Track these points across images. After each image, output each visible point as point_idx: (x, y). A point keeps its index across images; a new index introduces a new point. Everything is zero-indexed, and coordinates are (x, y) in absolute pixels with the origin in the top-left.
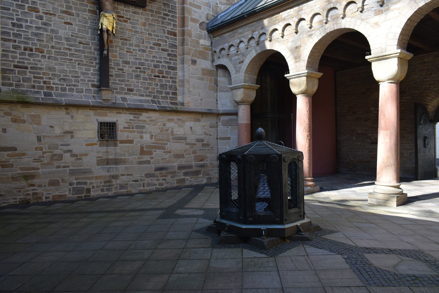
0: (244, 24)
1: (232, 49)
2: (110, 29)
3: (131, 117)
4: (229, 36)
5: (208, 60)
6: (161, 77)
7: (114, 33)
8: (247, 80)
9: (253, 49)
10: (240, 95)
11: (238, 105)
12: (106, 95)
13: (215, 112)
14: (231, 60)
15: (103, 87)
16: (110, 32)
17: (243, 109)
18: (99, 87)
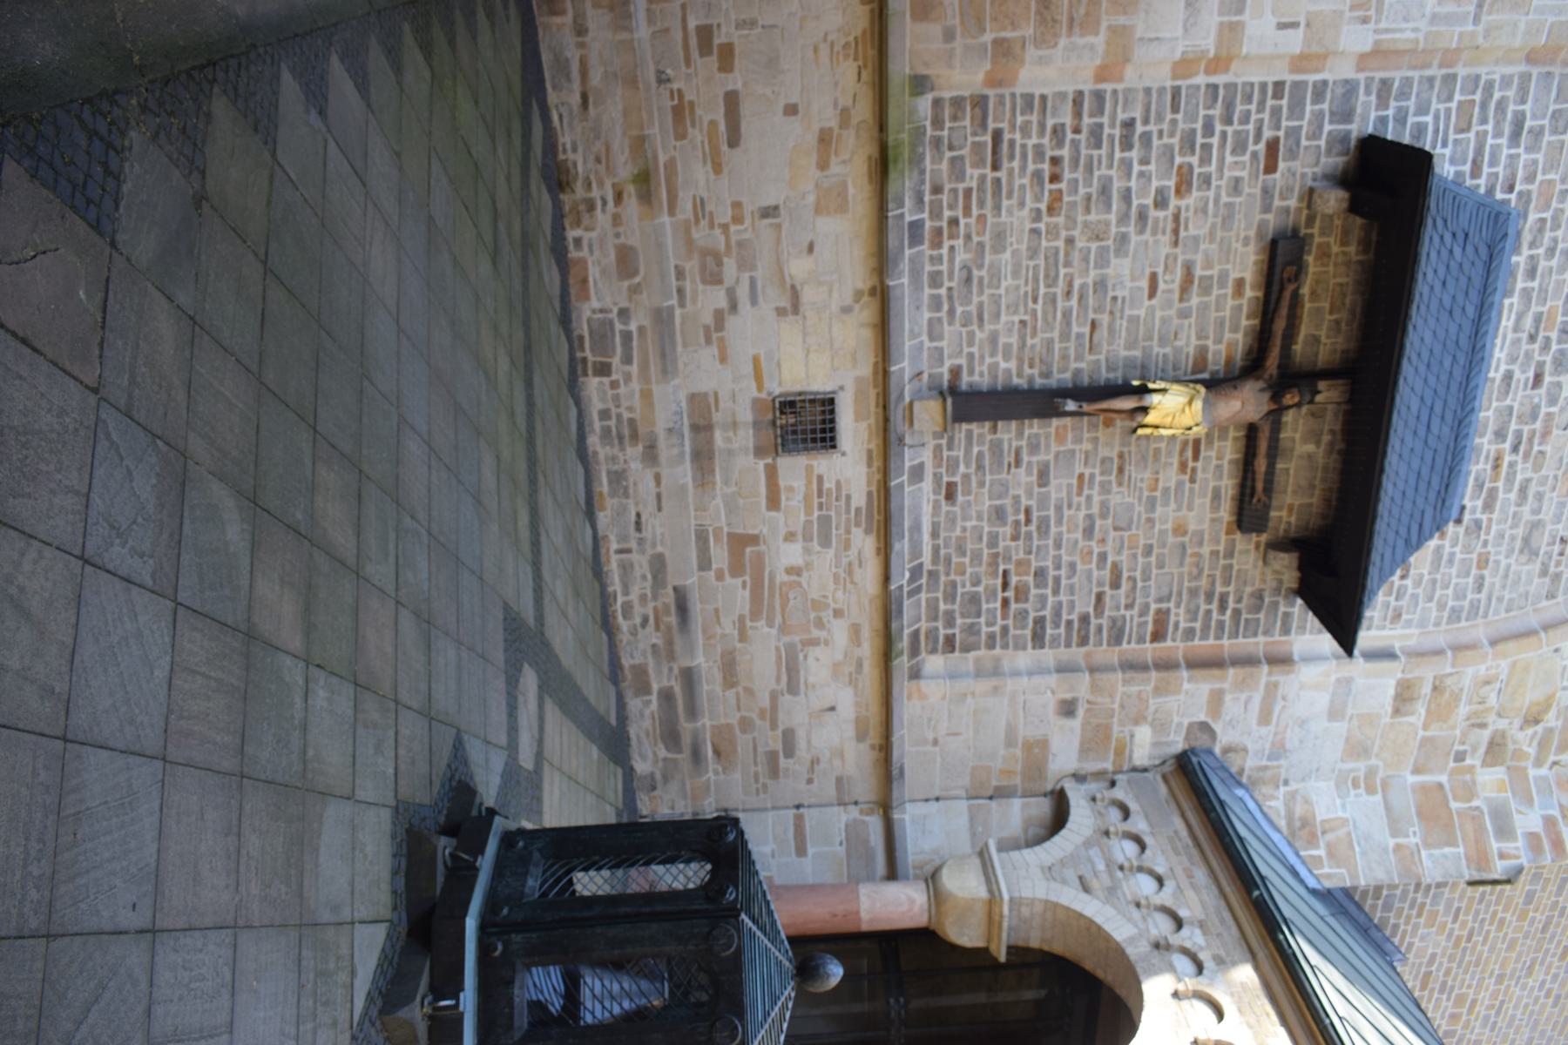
0: (1228, 890)
1: (1130, 848)
2: (1151, 418)
3: (859, 500)
5: (1080, 760)
6: (1006, 594)
7: (1140, 432)
8: (1019, 910)
9: (1136, 926)
10: (964, 884)
11: (926, 881)
12: (929, 413)
13: (895, 794)
14: (1088, 844)
16: (1139, 418)
17: (912, 901)
18: (953, 390)
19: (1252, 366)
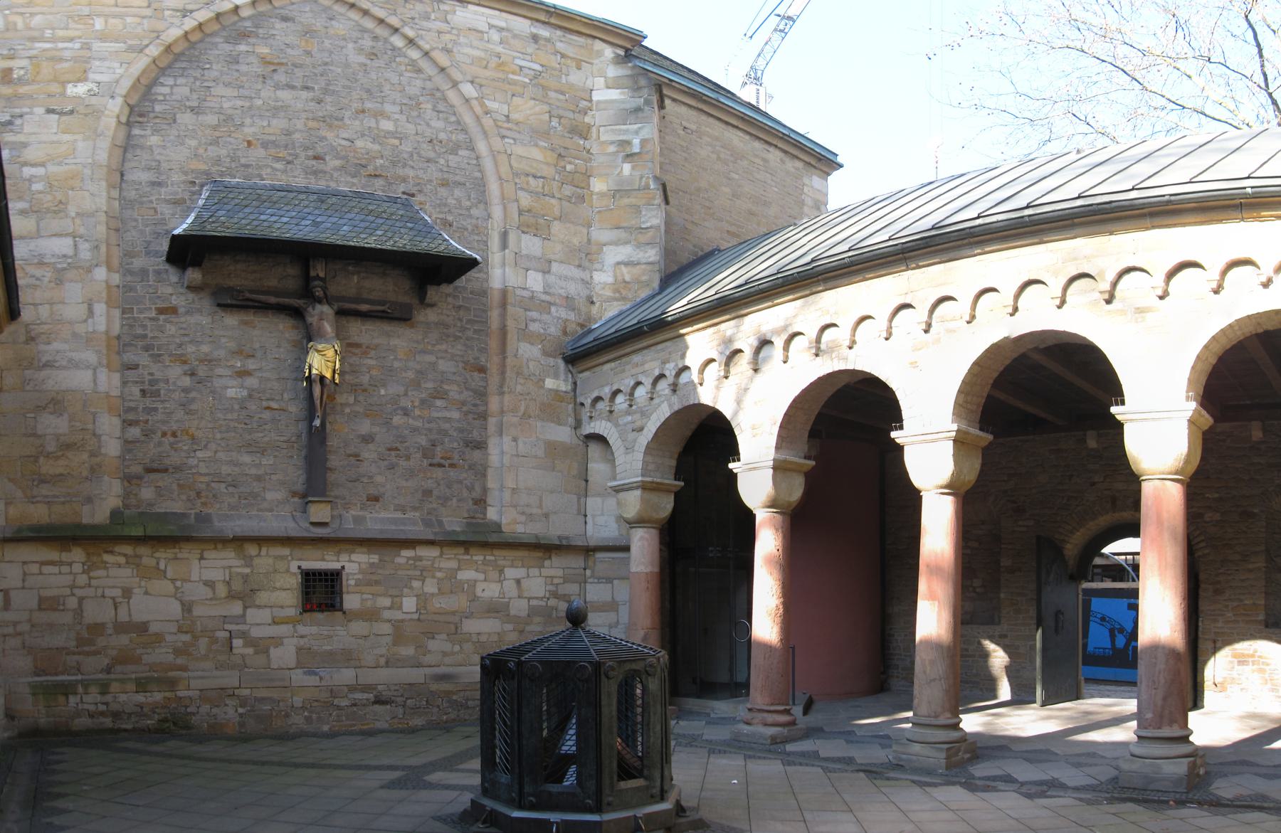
0: (645, 344)
2: (328, 375)
3: (375, 558)
4: (612, 370)
7: (337, 381)
12: (320, 512)
15: (313, 496)
16: (328, 382)
18: (304, 496)
19: (297, 314)
